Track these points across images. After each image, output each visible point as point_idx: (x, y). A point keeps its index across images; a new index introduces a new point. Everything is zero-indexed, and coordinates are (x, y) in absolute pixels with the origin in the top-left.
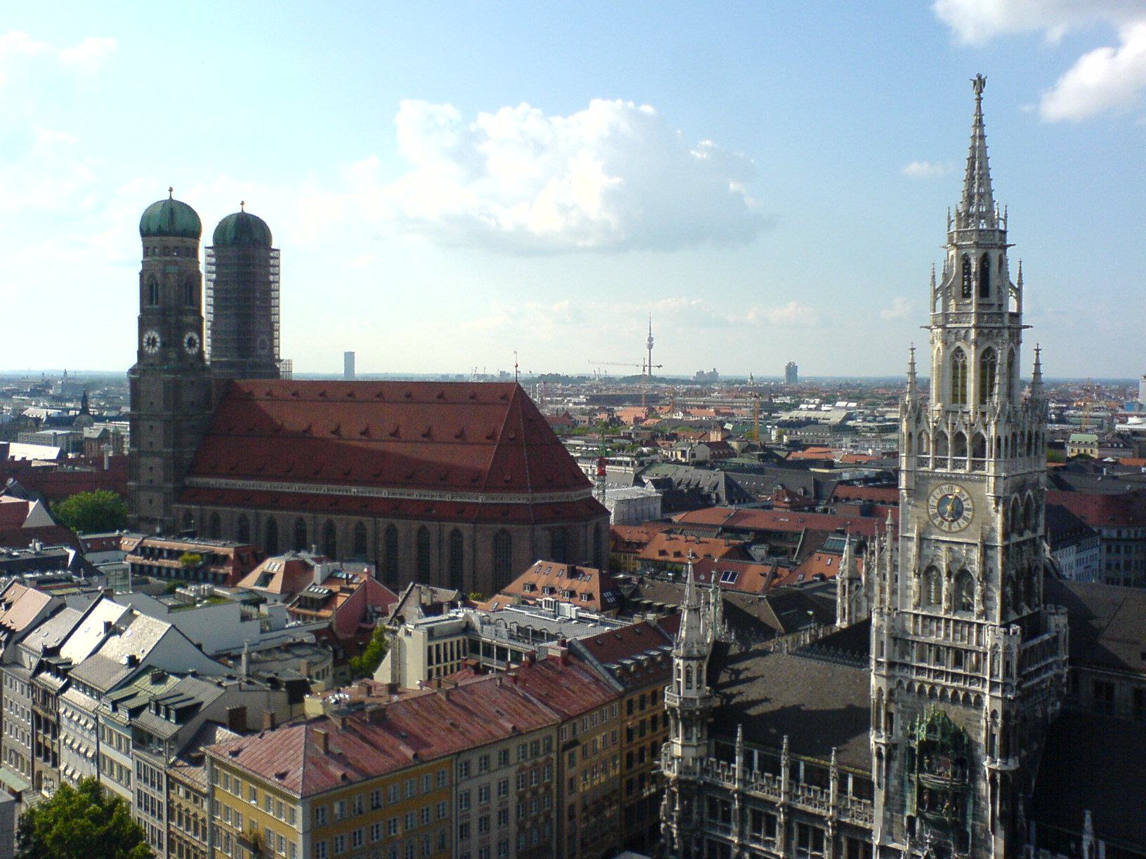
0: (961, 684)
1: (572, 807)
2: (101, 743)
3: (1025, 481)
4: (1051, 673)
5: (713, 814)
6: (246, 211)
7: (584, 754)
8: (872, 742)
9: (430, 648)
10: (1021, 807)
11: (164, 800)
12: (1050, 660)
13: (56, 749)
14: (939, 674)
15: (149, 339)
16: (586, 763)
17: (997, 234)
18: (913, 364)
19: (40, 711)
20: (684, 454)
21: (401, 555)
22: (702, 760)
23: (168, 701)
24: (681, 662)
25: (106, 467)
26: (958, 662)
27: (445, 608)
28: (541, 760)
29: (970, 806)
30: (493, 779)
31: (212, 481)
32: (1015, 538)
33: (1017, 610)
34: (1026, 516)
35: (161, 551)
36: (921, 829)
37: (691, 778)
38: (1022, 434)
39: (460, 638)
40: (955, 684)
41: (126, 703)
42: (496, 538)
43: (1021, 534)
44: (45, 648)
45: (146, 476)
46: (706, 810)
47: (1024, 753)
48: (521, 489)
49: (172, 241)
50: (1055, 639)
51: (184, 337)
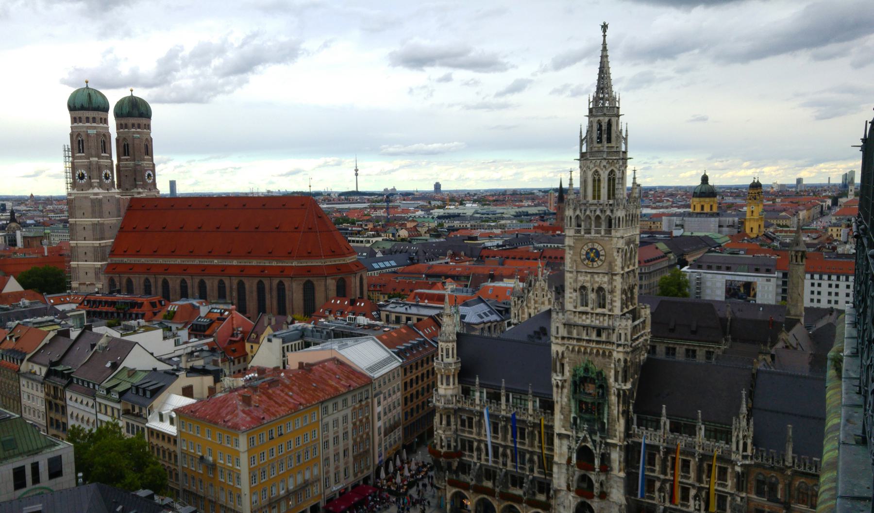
0: (601, 346)
1: (379, 428)
2: (98, 414)
3: (630, 239)
5: (463, 424)
6: (134, 95)
7: (385, 398)
8: (553, 379)
9: (283, 348)
10: (631, 407)
12: (643, 332)
13: (64, 420)
14: (588, 341)
15: (79, 175)
16: (386, 402)
17: (616, 109)
18: (571, 179)
19: (51, 398)
20: (393, 235)
21: (247, 298)
22: (456, 396)
24: (443, 344)
25: (46, 254)
26: (599, 335)
28: (363, 403)
29: (606, 409)
30: (339, 415)
31: (126, 260)
32: (626, 270)
34: (630, 259)
35: (100, 302)
36: (580, 423)
37: (450, 406)
39: (300, 341)
40: (597, 346)
41: (116, 389)
42: (305, 285)
43: (628, 268)
44: (51, 361)
46: (459, 423)
48: (318, 257)
49: (91, 114)
51: (102, 173)
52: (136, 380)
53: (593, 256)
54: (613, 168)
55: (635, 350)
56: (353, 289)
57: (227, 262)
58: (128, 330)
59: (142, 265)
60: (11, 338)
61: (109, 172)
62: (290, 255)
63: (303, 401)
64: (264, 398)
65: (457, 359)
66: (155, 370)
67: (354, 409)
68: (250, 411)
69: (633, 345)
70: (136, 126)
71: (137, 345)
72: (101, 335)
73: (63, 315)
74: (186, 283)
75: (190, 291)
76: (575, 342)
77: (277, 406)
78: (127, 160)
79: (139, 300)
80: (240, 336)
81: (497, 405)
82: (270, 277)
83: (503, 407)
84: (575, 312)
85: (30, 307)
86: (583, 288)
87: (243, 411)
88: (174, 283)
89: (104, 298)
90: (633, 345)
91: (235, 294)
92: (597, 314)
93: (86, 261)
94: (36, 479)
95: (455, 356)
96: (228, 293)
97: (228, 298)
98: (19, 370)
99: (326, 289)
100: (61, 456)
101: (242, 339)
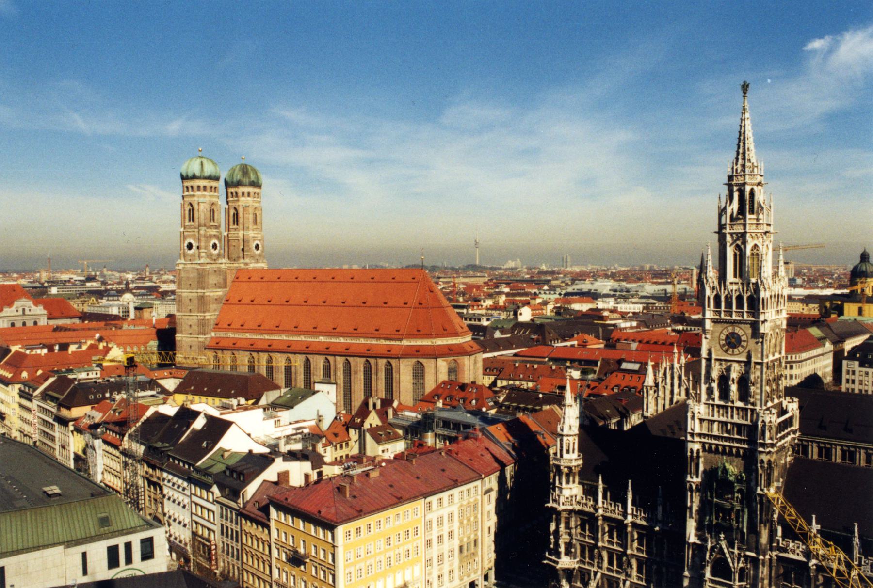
11: (239, 530)
30: (445, 512)
31: (231, 335)
38: (775, 296)
43: (774, 355)
48: (428, 336)
50: (791, 418)
52: (231, 462)
54: (756, 242)
56: (466, 373)
57: (333, 340)
58: (228, 408)
59: (247, 339)
61: (217, 242)
65: (579, 456)
66: (250, 451)
67: (461, 506)
70: (246, 194)
71: (234, 425)
78: (235, 229)
84: (713, 405)
93: (191, 334)
94: (129, 560)
95: (576, 451)
97: (332, 377)
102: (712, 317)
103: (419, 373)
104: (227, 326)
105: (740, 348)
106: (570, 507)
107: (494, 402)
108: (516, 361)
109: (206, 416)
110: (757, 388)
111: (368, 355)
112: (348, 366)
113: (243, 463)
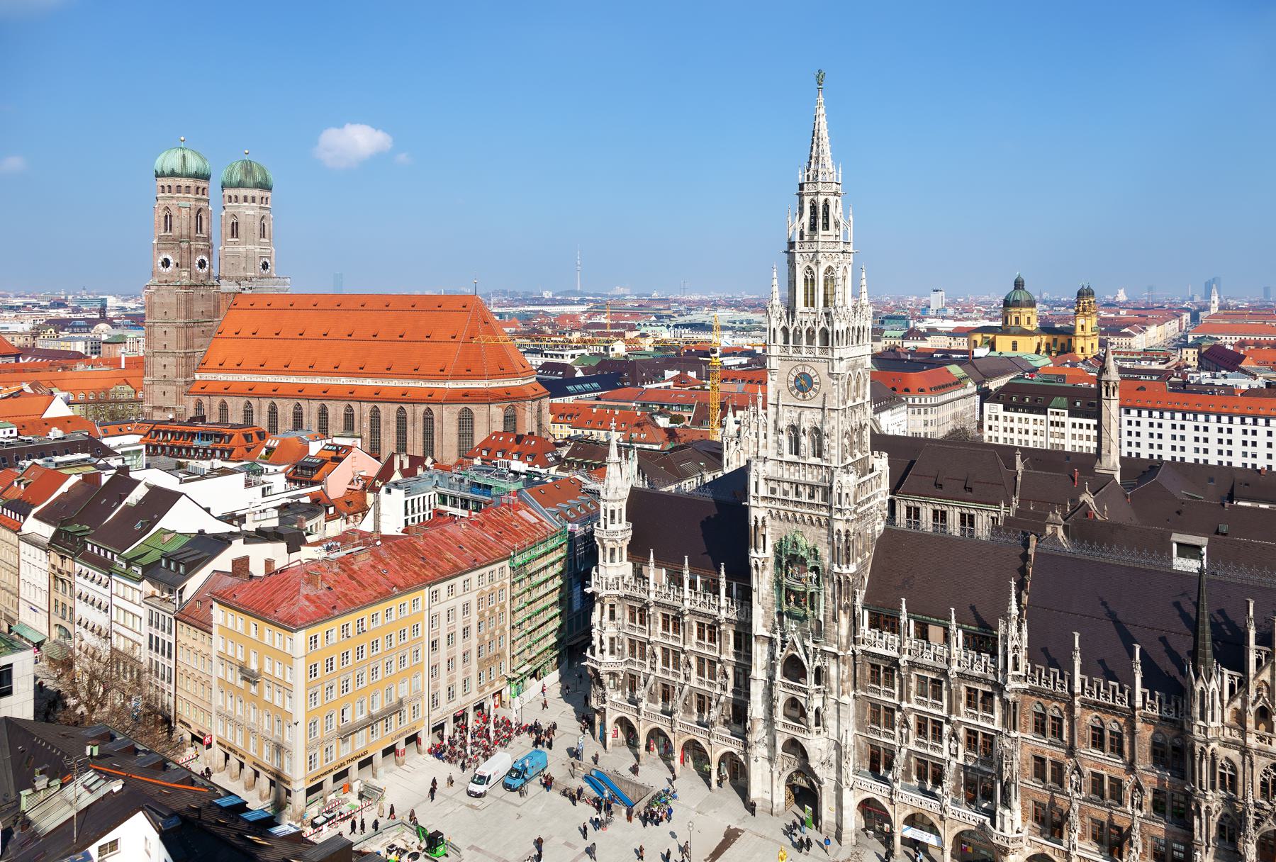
4: (877, 501)
9: (406, 502)
20: (606, 349)
23: (179, 557)
27: (420, 471)
30: (458, 603)
33: (853, 456)
45: (159, 372)
47: (859, 560)
48: (480, 376)
52: (171, 549)
53: (803, 384)
55: (862, 517)
60: (19, 483)
62: (442, 374)
63: (401, 582)
64: (345, 575)
66: (201, 532)
68: (318, 597)
69: (859, 511)
72: (137, 482)
73: (109, 452)
74: (301, 408)
75: (305, 420)
76: (779, 505)
77: (360, 589)
79: (228, 431)
80: (361, 483)
81: (678, 591)
82: (414, 402)
83: (687, 595)
84: (781, 462)
85: (63, 439)
86: (794, 429)
87: (307, 597)
88: (286, 409)
89: (180, 429)
90: (859, 511)
91: (366, 425)
92: (810, 465)
96: (356, 424)
98: (20, 530)
99: (490, 420)
100: (11, 665)
101: (364, 487)
102: (779, 353)
103: (466, 422)
104: (217, 366)
105: (811, 392)
106: (616, 592)
107: (556, 457)
108: (594, 406)
109: (146, 485)
110: (832, 441)
111: (404, 398)
112: (375, 417)
113: (188, 549)
